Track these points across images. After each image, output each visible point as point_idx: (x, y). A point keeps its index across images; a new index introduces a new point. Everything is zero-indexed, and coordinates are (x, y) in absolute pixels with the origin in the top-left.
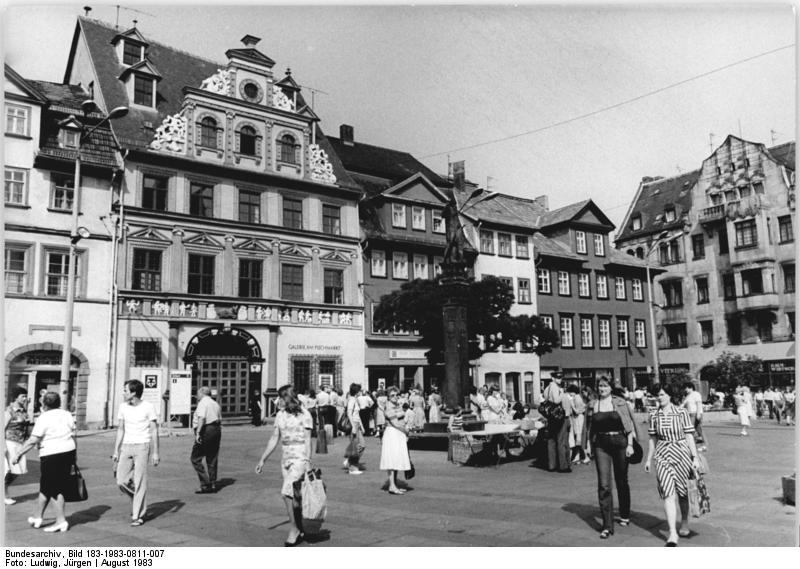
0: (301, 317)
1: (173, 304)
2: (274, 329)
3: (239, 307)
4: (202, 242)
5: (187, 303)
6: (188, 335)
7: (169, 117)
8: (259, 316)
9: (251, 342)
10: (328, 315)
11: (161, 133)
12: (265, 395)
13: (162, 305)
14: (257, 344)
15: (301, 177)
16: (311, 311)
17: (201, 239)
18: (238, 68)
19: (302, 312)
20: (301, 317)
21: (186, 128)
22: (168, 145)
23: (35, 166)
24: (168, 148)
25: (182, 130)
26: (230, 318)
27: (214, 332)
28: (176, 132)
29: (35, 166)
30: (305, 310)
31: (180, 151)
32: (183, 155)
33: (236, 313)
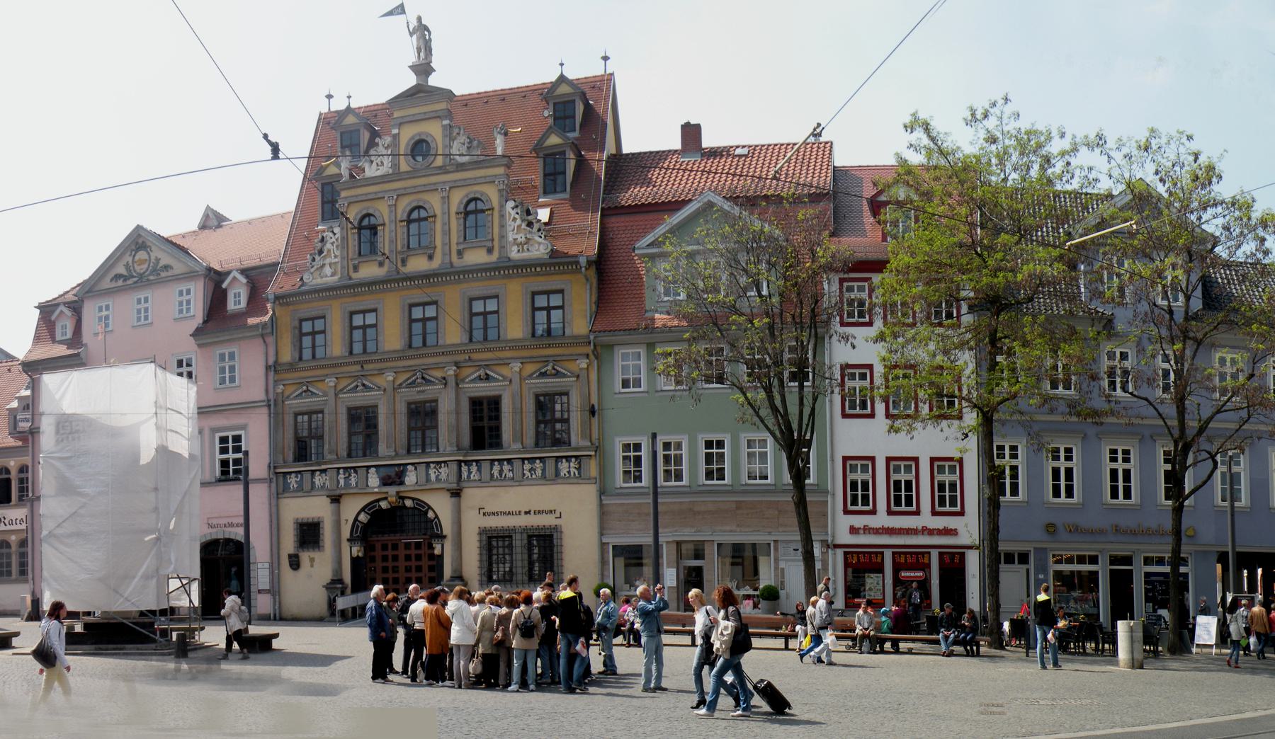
0: (496, 473)
2: (456, 494)
6: (352, 509)
8: (433, 477)
10: (538, 464)
18: (401, 124)
20: (496, 473)
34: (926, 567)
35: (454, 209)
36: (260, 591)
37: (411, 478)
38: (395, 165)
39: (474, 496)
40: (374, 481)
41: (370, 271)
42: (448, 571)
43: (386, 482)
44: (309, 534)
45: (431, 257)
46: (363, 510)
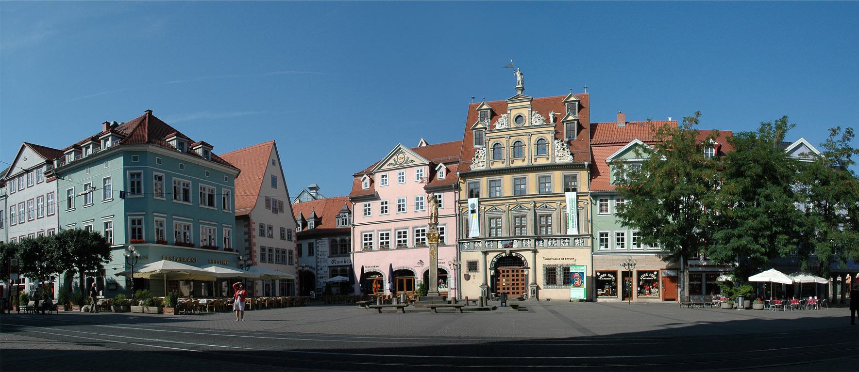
6: (491, 257)
10: (567, 241)
15: (549, 162)
32: (484, 168)
34: (700, 280)
37: (516, 245)
38: (509, 125)
39: (542, 252)
40: (500, 246)
41: (498, 165)
42: (531, 281)
44: (473, 266)
45: (524, 160)
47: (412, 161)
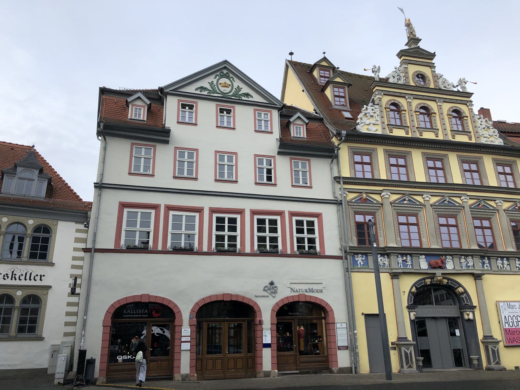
1: (392, 257)
2: (477, 277)
3: (446, 258)
4: (405, 202)
5: (402, 255)
6: (407, 284)
7: (365, 106)
8: (464, 265)
9: (460, 290)
11: (361, 119)
12: (483, 342)
13: (382, 258)
14: (466, 292)
16: (508, 259)
17: (405, 200)
19: (499, 261)
20: (500, 265)
21: (378, 113)
22: (367, 127)
23: (279, 153)
24: (368, 129)
25: (376, 115)
26: (440, 267)
27: (428, 281)
28: (372, 116)
29: (278, 154)
30: (502, 258)
31: (377, 130)
32: (380, 132)
33: (443, 262)
35: (445, 112)
36: (339, 348)
40: (424, 265)
43: (431, 266)
46: (414, 285)
47: (247, 95)
